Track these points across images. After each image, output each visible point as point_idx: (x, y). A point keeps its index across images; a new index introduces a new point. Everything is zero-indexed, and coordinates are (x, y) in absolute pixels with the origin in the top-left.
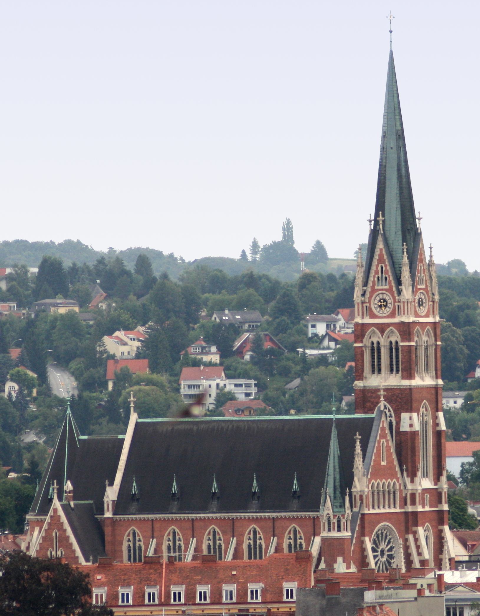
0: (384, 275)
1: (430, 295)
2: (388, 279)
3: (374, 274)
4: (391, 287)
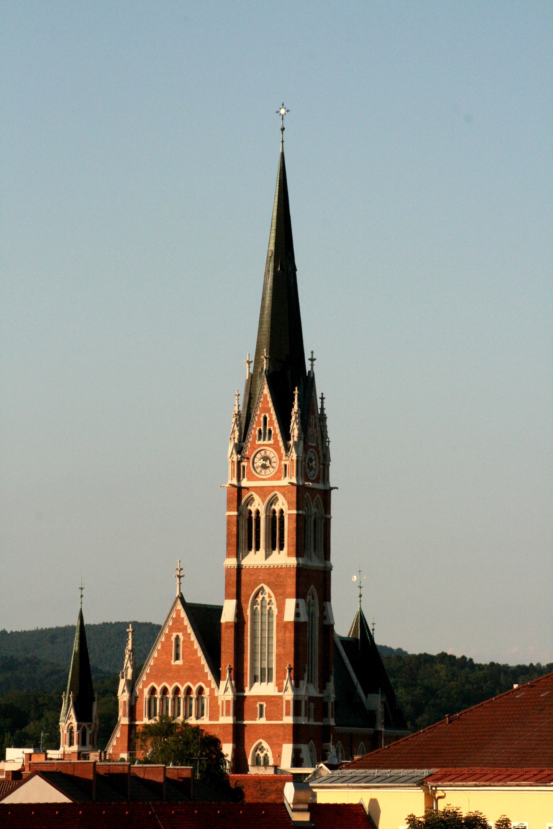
0: (268, 428)
2: (273, 432)
4: (276, 441)
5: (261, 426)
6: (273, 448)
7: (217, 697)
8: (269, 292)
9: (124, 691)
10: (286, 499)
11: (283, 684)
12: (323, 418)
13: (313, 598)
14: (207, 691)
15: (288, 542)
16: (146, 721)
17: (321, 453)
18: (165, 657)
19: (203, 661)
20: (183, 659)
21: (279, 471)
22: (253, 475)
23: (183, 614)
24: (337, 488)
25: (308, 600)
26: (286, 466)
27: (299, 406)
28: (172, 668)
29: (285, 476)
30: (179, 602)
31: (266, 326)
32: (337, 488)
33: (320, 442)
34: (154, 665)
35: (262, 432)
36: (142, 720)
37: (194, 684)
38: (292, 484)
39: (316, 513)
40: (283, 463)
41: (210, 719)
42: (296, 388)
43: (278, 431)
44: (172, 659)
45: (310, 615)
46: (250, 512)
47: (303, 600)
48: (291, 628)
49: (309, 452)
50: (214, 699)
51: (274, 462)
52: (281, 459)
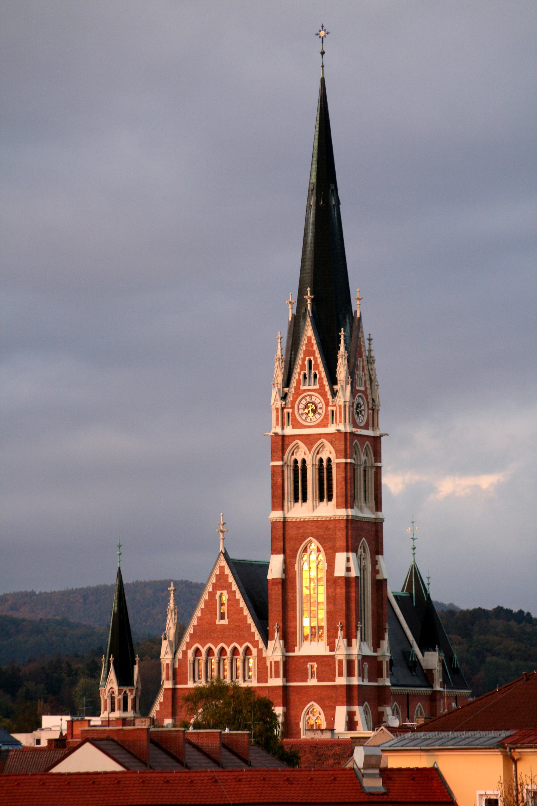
0: (313, 372)
1: (370, 401)
2: (318, 376)
3: (298, 370)
4: (322, 386)
5: (305, 370)
6: (319, 393)
7: (265, 658)
8: (311, 227)
9: (166, 653)
10: (333, 447)
11: (334, 643)
12: (370, 361)
13: (365, 552)
14: (254, 651)
15: (337, 493)
16: (190, 685)
17: (370, 397)
18: (209, 616)
19: (250, 621)
20: (228, 618)
21: (326, 416)
22: (299, 422)
23: (227, 571)
24: (387, 435)
25: (359, 554)
26: (333, 412)
27: (346, 348)
28: (216, 628)
29: (332, 423)
30: (222, 558)
31: (309, 264)
32: (387, 435)
33: (368, 386)
34: (198, 625)
35: (307, 376)
36: (186, 683)
37: (241, 645)
38: (339, 431)
39: (365, 461)
40: (330, 409)
41: (259, 682)
42: (342, 329)
43: (323, 374)
44: (216, 618)
45: (362, 569)
46: (296, 461)
47: (354, 554)
48: (342, 583)
49: (356, 397)
50: (261, 660)
51: (321, 408)
52: (327, 405)
